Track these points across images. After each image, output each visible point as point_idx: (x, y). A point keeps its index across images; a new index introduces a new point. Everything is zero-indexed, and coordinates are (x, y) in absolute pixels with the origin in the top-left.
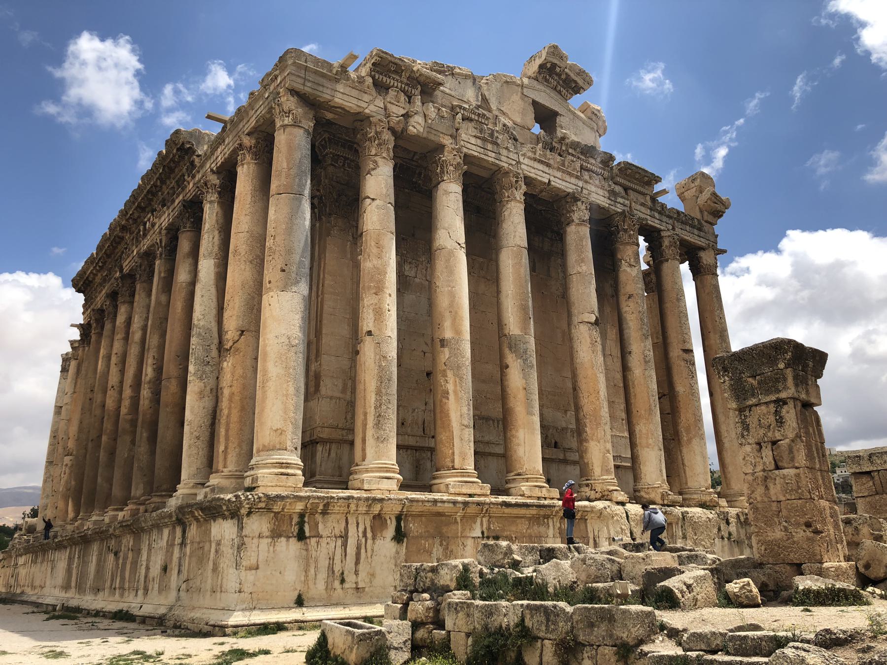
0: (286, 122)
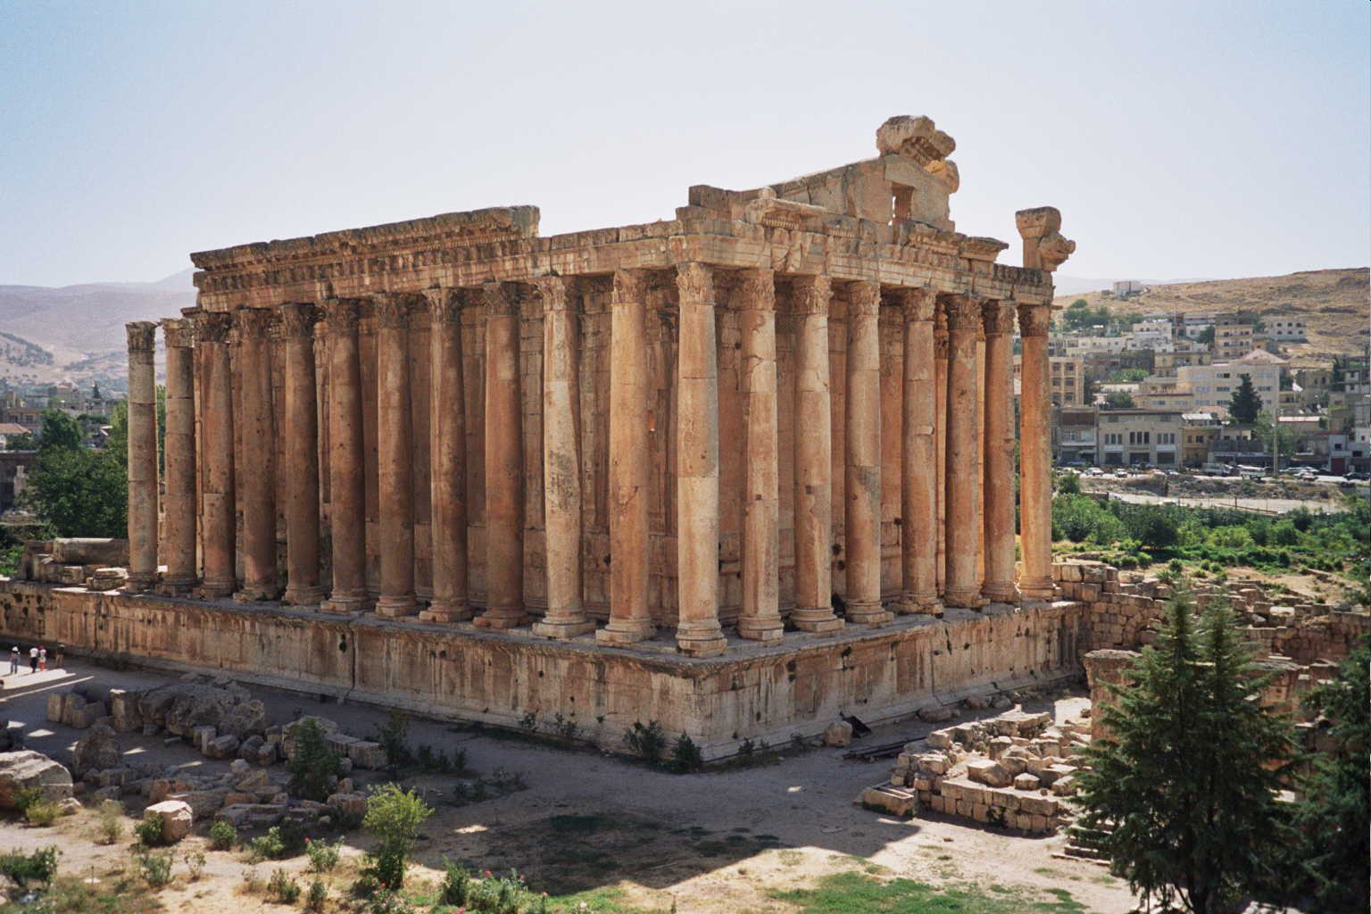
0: (697, 298)
